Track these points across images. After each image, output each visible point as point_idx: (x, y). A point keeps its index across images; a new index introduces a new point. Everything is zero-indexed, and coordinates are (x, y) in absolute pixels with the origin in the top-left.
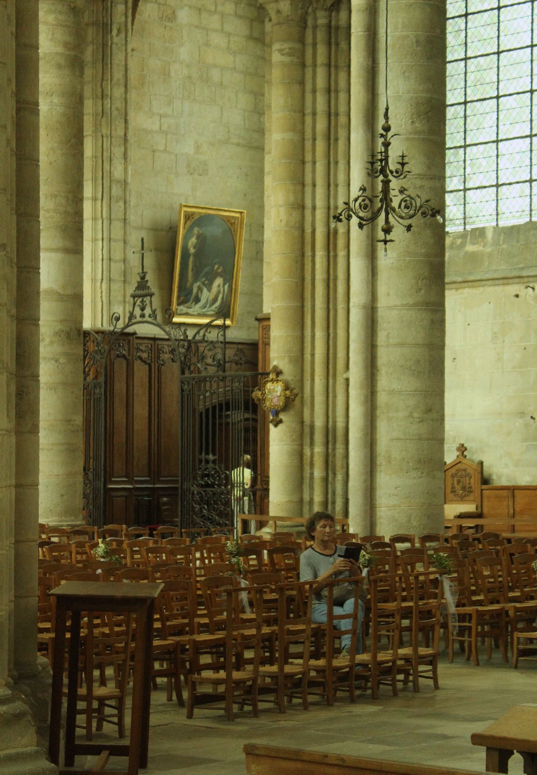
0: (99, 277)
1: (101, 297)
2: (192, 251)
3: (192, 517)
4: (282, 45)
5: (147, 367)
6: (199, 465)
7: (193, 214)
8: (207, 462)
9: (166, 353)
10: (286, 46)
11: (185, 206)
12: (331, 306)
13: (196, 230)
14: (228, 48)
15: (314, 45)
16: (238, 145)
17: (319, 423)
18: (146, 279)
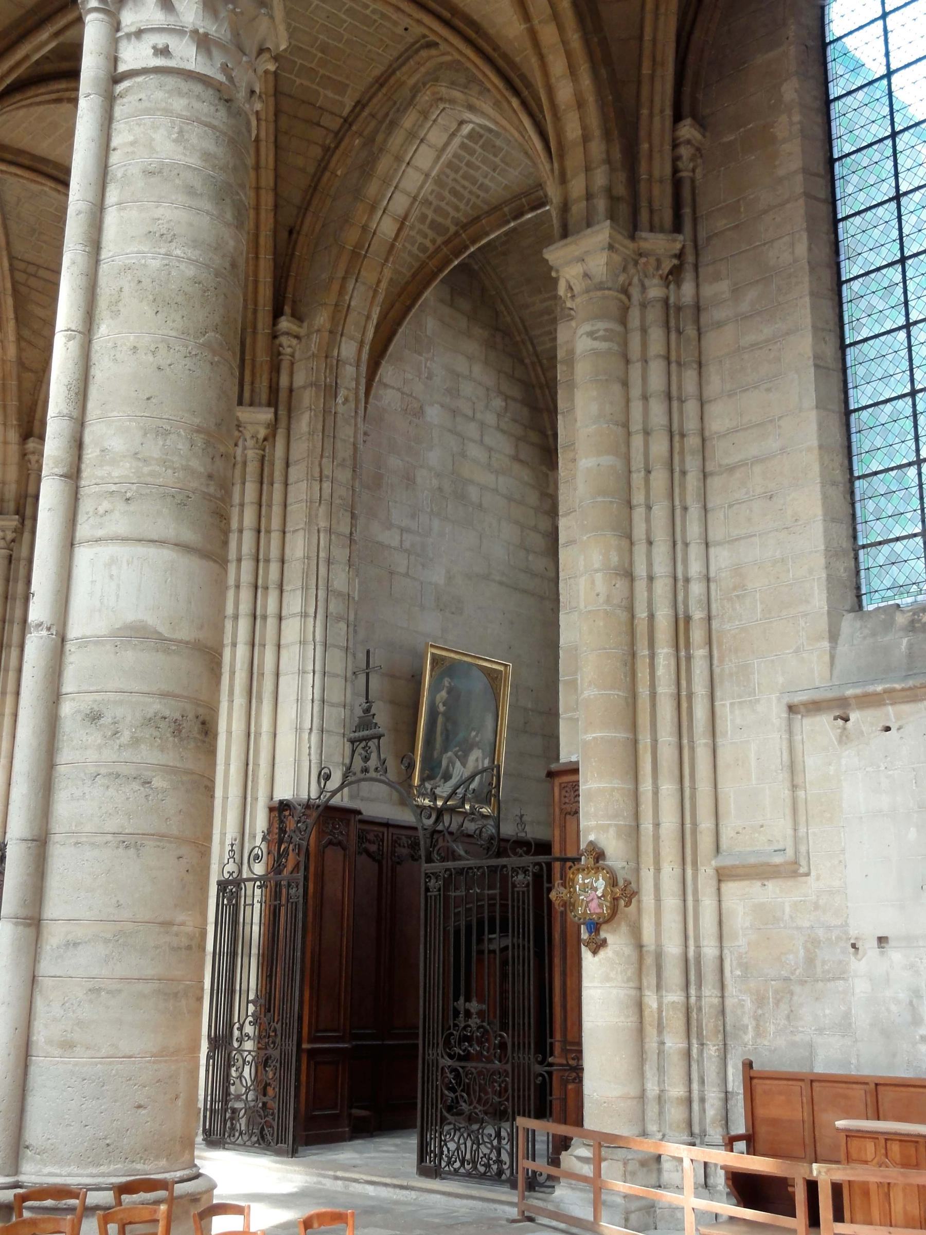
0: (307, 725)
1: (309, 754)
2: (442, 708)
3: (441, 1112)
4: (593, 325)
5: (376, 865)
6: (454, 1020)
7: (443, 659)
8: (468, 1014)
9: (404, 847)
10: (601, 326)
11: (432, 646)
12: (685, 741)
13: (446, 682)
14: (489, 465)
15: (644, 331)
16: (501, 583)
17: (672, 948)
18: (372, 713)
